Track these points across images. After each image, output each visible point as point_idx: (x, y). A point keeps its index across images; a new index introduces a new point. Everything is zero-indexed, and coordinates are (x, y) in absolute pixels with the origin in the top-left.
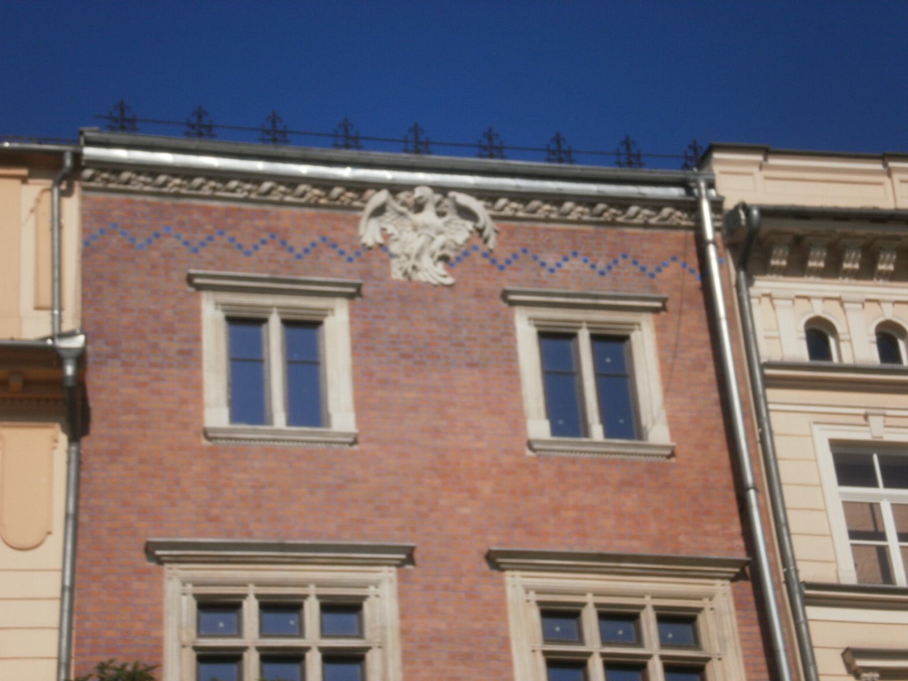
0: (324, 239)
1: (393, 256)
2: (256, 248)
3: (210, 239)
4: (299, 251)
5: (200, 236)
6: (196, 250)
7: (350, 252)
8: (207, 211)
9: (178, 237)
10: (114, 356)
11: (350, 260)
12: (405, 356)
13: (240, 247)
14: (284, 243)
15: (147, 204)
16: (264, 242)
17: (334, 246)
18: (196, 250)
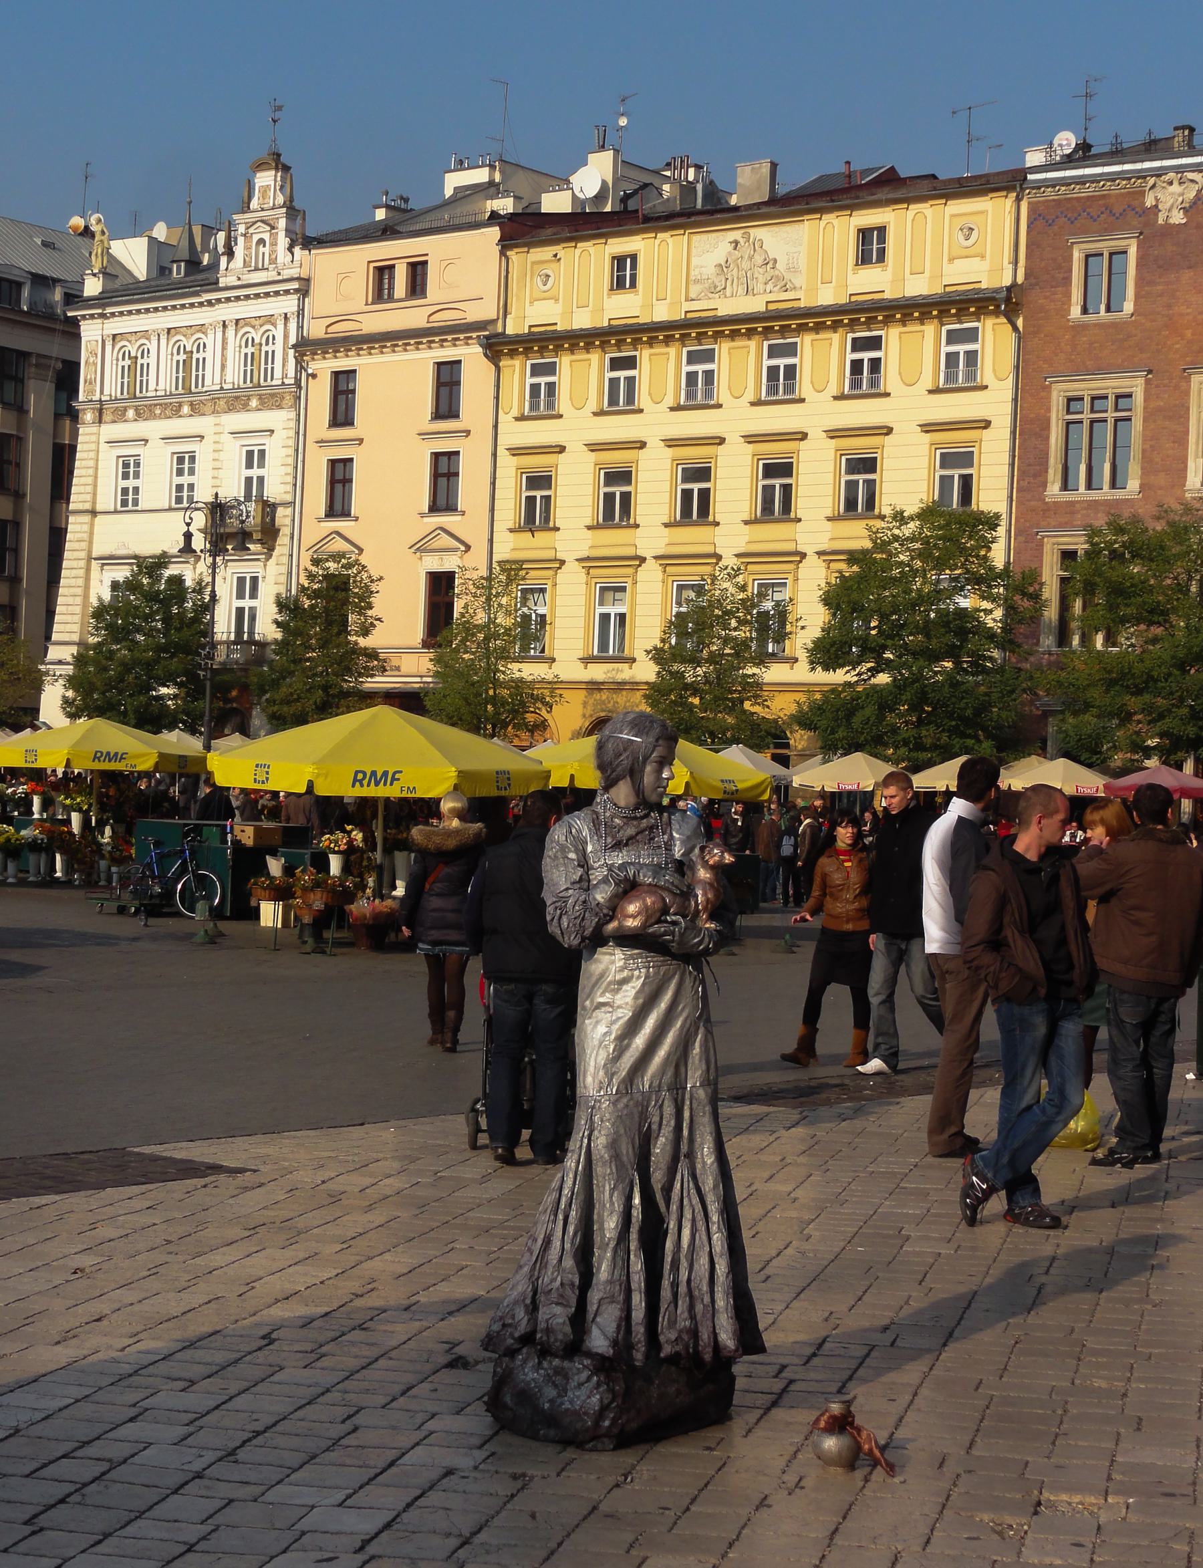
0: (1129, 206)
1: (1160, 211)
2: (1099, 216)
3: (1079, 215)
4: (1117, 215)
5: (1076, 215)
6: (1072, 223)
7: (1141, 212)
8: (1078, 199)
9: (1066, 217)
10: (1037, 284)
11: (1140, 216)
12: (1160, 267)
13: (1091, 217)
14: (1111, 212)
15: (1054, 200)
16: (1102, 213)
17: (1133, 209)
18: (1072, 223)
